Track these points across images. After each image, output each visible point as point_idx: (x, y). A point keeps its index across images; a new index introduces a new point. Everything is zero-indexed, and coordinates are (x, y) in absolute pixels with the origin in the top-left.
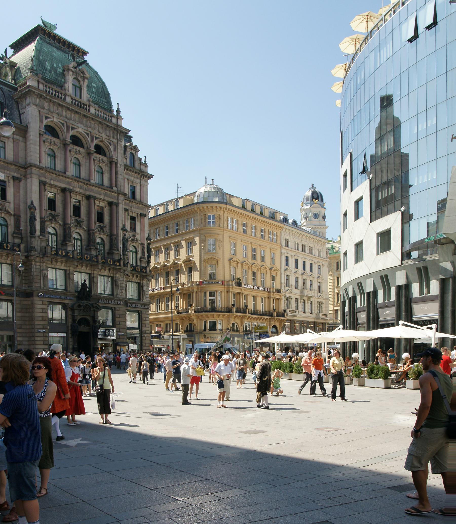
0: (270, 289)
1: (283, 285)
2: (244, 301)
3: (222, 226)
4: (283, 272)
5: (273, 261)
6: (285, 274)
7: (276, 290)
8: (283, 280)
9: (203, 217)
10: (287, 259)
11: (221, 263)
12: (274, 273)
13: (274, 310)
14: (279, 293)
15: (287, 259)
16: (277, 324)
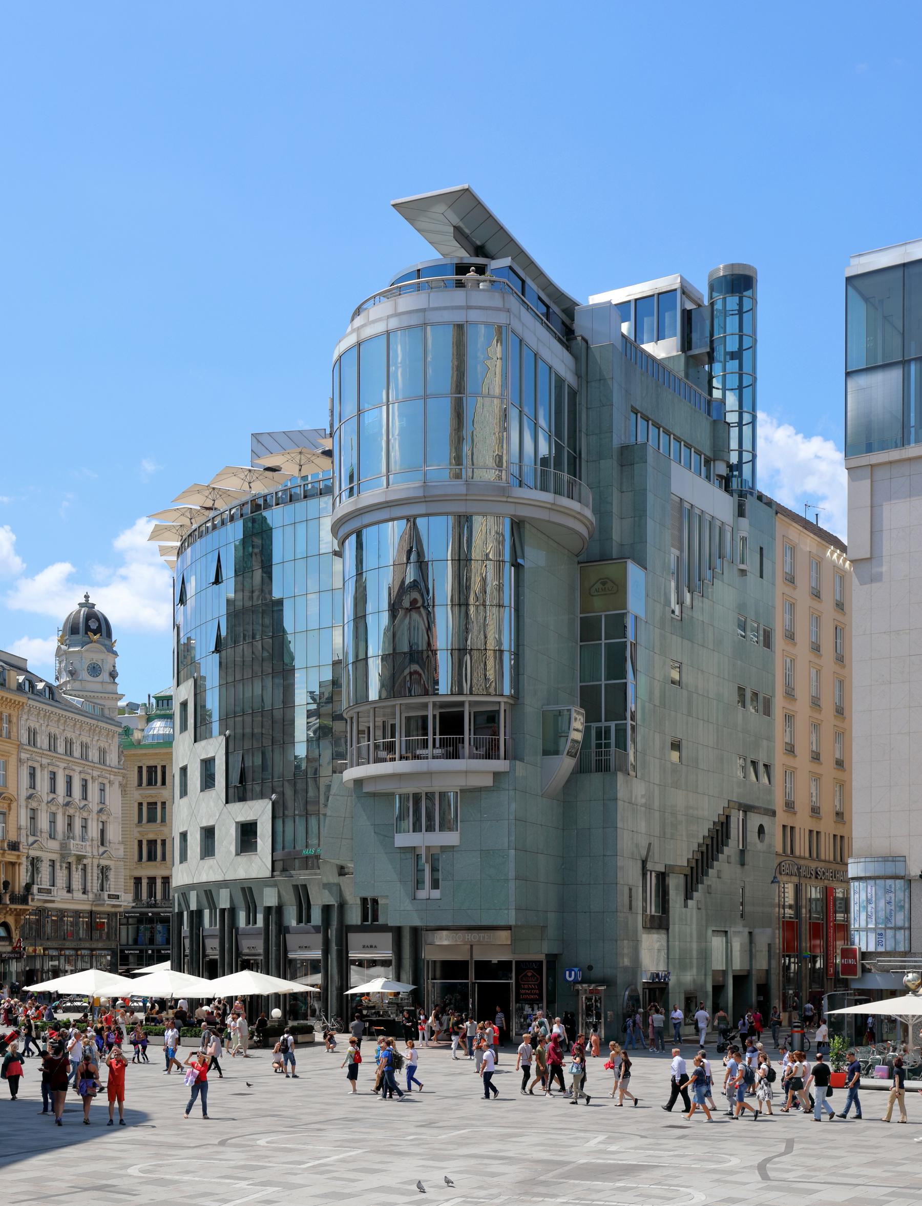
1: (23, 832)
4: (23, 802)
7: (8, 845)
8: (24, 821)
14: (15, 850)
16: (10, 920)
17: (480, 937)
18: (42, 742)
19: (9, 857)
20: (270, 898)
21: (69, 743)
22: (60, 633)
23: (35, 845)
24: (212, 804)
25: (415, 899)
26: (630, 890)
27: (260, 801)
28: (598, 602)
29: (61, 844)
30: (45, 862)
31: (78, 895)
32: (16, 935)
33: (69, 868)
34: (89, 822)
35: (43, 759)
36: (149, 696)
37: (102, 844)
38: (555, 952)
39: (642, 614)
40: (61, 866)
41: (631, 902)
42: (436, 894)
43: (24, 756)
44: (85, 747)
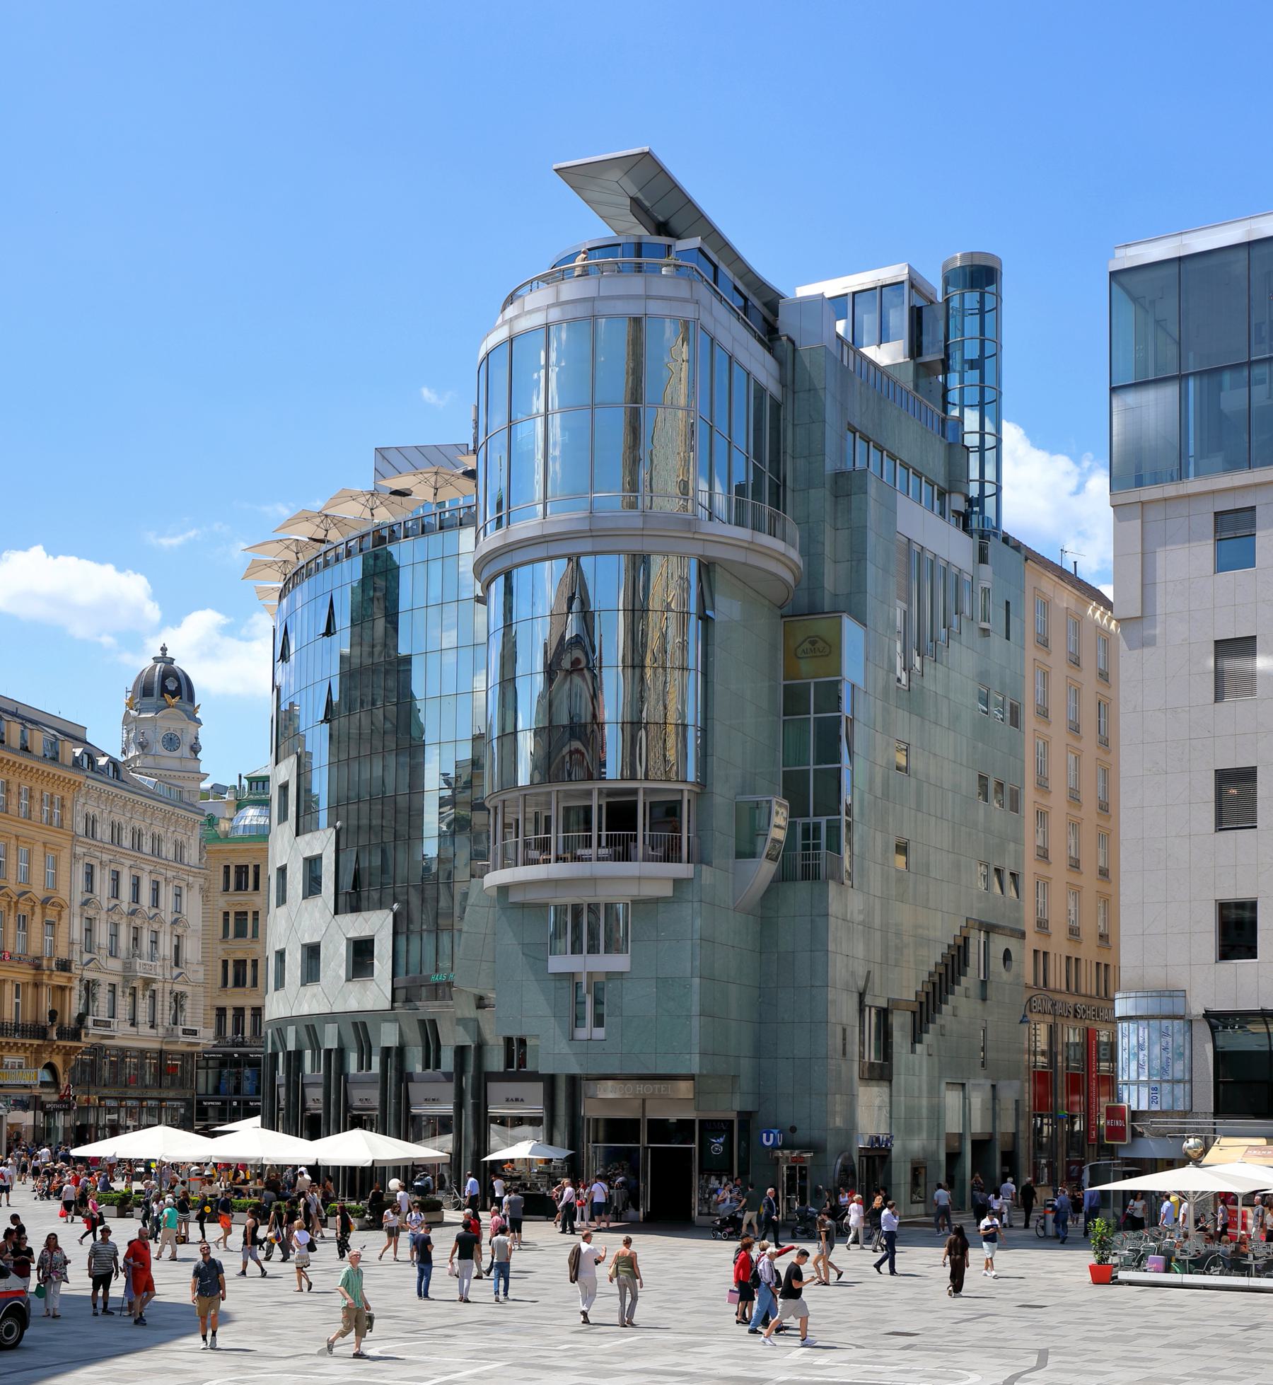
1: (77, 948)
4: (76, 909)
6: (81, 915)
7: (57, 964)
8: (78, 933)
16: (58, 1061)
17: (654, 1089)
18: (103, 833)
19: (56, 979)
20: (388, 1036)
21: (137, 835)
22: (129, 695)
23: (91, 965)
24: (317, 915)
25: (572, 1039)
26: (844, 1030)
27: (378, 912)
28: (805, 666)
29: (125, 963)
30: (103, 986)
31: (144, 1029)
32: (64, 1080)
33: (134, 994)
34: (161, 936)
35: (104, 855)
36: (240, 776)
37: (177, 964)
38: (750, 1109)
39: (860, 683)
40: (123, 992)
41: (844, 1045)
42: (600, 1033)
43: (79, 850)
44: (157, 840)
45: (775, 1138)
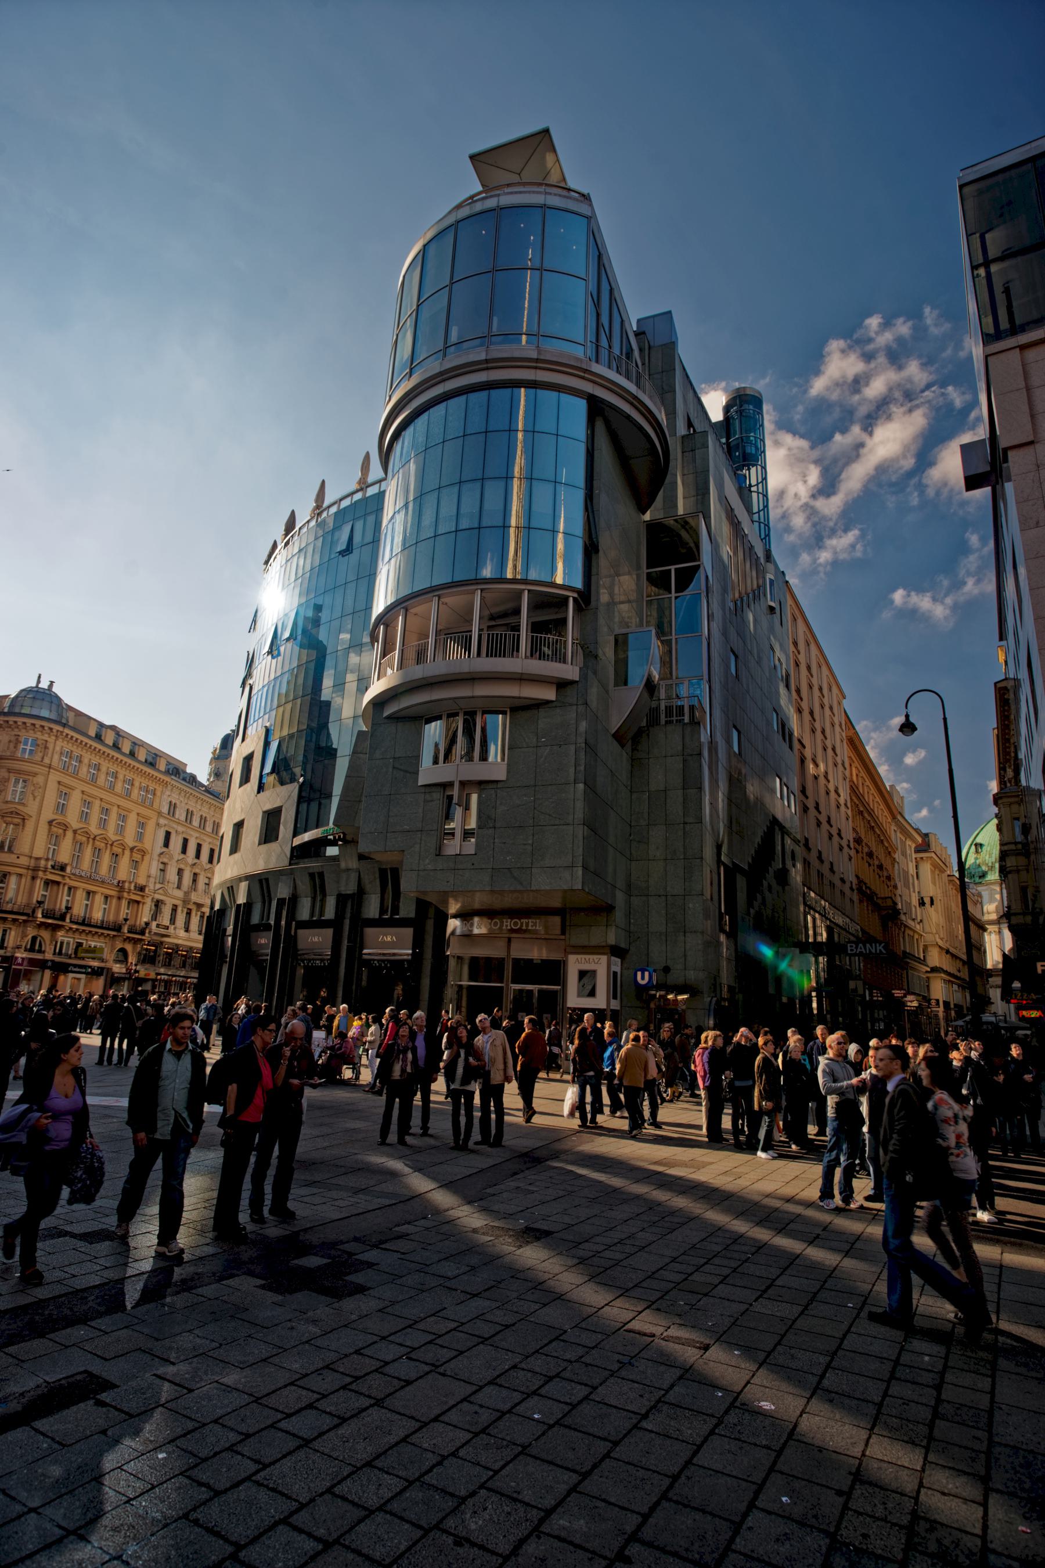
0: (124, 882)
1: (152, 880)
2: (66, 898)
3: (47, 761)
5: (140, 837)
7: (135, 887)
9: (13, 738)
10: (168, 835)
11: (30, 825)
12: (137, 857)
13: (126, 920)
15: (168, 835)
16: (129, 947)
18: (180, 815)
45: (650, 977)
